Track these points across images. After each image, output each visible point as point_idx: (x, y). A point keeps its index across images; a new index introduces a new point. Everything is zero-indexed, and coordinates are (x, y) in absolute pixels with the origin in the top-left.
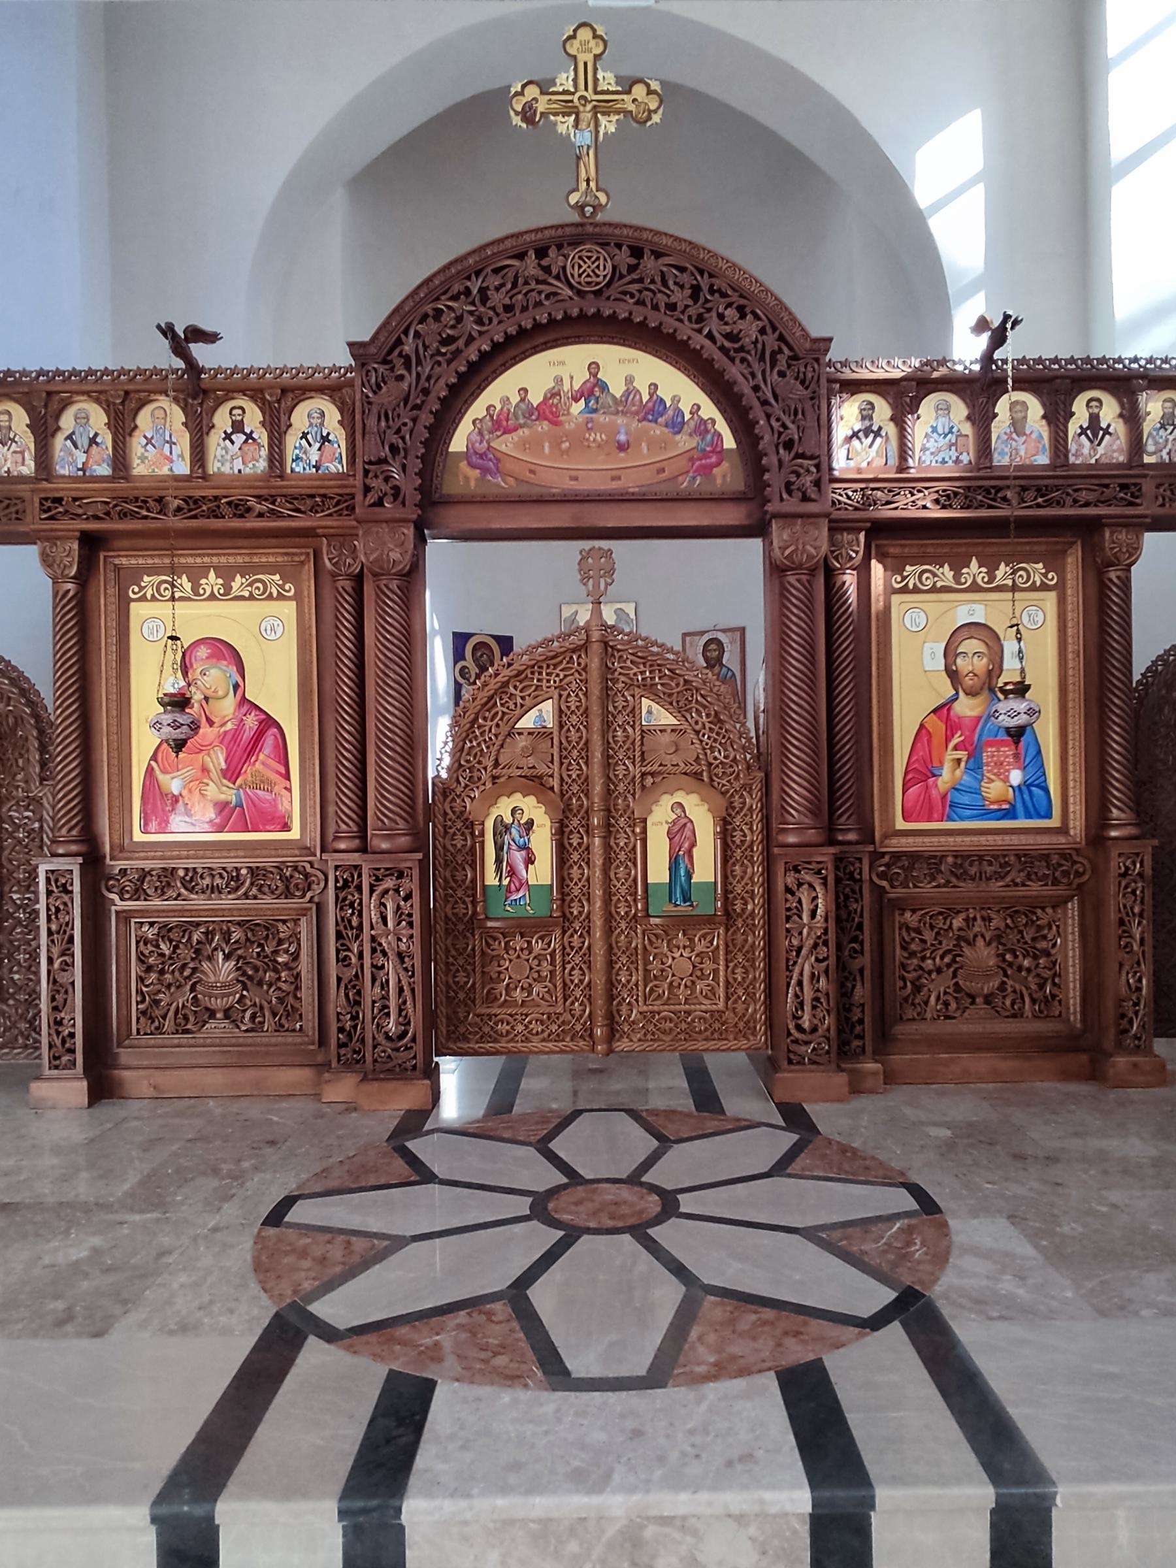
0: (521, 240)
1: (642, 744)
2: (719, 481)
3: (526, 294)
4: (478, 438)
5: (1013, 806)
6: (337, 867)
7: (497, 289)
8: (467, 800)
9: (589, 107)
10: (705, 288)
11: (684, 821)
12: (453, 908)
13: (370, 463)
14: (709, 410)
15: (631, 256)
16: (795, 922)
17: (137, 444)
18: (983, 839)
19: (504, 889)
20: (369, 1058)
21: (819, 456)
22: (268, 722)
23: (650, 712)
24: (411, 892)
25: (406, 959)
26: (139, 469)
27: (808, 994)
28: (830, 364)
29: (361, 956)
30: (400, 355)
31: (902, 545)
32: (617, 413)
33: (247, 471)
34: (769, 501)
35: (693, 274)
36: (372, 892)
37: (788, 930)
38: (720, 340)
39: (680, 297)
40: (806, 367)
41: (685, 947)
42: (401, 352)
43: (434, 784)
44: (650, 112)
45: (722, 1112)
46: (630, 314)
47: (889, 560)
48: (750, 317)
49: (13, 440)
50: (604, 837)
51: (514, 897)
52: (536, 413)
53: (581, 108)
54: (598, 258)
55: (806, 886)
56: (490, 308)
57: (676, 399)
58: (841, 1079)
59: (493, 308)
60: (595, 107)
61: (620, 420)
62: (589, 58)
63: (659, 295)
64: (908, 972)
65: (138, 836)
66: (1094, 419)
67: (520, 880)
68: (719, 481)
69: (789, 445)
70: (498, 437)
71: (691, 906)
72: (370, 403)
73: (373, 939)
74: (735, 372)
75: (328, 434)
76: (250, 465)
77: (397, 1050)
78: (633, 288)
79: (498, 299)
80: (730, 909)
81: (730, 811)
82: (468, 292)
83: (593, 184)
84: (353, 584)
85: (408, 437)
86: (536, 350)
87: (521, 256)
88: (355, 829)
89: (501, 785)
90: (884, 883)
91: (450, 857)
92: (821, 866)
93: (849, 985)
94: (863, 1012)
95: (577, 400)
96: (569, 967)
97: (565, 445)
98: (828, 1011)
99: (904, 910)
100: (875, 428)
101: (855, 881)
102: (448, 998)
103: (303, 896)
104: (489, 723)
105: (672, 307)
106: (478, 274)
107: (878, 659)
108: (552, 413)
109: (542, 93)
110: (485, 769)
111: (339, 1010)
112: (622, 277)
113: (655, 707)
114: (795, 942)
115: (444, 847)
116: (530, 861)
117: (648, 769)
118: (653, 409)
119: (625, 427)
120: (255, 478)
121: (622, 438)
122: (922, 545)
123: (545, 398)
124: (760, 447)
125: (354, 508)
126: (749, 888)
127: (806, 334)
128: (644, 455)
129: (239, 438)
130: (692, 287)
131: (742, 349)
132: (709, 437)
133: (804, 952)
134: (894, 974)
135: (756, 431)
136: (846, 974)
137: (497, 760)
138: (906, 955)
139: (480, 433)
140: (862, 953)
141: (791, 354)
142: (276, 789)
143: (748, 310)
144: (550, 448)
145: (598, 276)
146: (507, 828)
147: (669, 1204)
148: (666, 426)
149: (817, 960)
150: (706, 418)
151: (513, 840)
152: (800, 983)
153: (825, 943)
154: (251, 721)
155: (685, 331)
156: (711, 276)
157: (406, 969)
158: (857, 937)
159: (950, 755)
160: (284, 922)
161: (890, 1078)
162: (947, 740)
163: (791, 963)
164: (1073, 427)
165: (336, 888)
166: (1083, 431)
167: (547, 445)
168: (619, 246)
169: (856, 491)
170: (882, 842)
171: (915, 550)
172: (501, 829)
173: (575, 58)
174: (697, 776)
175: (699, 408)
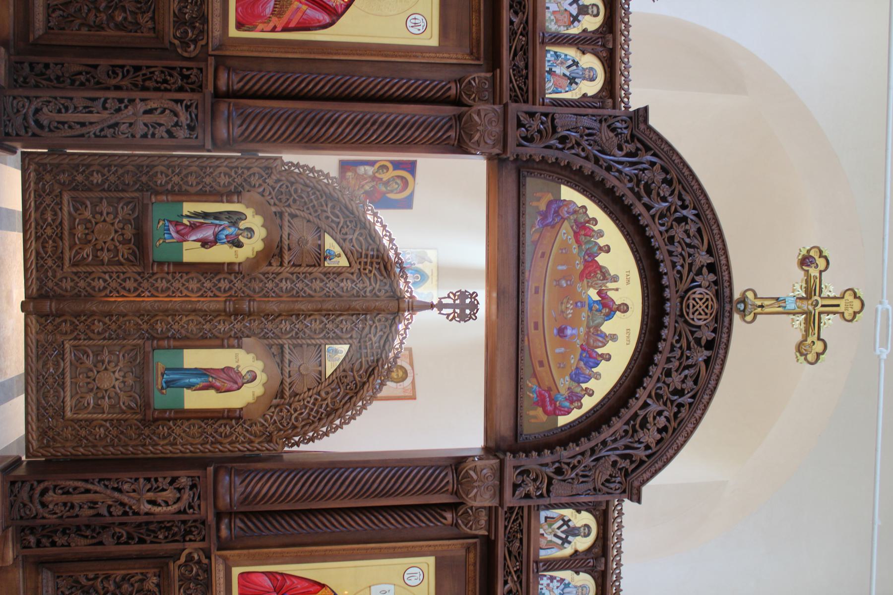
0: (721, 252)
1: (308, 345)
2: (532, 413)
3: (681, 254)
4: (571, 210)
6: (201, 70)
7: (686, 232)
8: (261, 190)
9: (811, 308)
10: (680, 400)
11: (240, 381)
12: (162, 173)
13: (553, 119)
14: (588, 403)
15: (707, 340)
16: (145, 485)
19: (178, 219)
20: (16, 92)
21: (549, 496)
24: (174, 137)
25: (112, 130)
27: (77, 499)
28: (621, 501)
29: (118, 88)
30: (638, 149)
31: (475, 563)
32: (588, 327)
33: (548, 14)
34: (514, 457)
35: (691, 390)
36: (177, 101)
37: (137, 479)
38: (642, 413)
39: (676, 380)
40: (619, 483)
41: (124, 382)
42: (641, 150)
43: (276, 159)
44: (806, 355)
46: (665, 340)
47: (464, 554)
48: (658, 436)
50: (225, 311)
51: (172, 229)
52: (590, 259)
53: (810, 302)
54: (706, 314)
55: (178, 495)
56: (672, 225)
57: (598, 376)
59: (672, 227)
60: (811, 312)
61: (582, 330)
62: (841, 309)
63: (677, 363)
64: (102, 582)
67: (187, 234)
68: (532, 413)
69: (559, 471)
70: (572, 227)
71: (162, 388)
72: (601, 122)
74: (618, 425)
75: (577, 84)
76: (552, 17)
77: (25, 118)
78: (684, 343)
79: (678, 232)
80: (160, 422)
81: (248, 423)
82: (684, 207)
83: (759, 310)
84: (453, 97)
85: (573, 151)
86: (638, 261)
88: (235, 87)
89: (273, 220)
90: (183, 559)
91: (208, 170)
92: (196, 508)
93: (88, 533)
94: (63, 545)
95: (599, 293)
96: (107, 277)
97: (564, 283)
98: (62, 517)
99: (159, 576)
100: (570, 538)
101: (184, 536)
102: (78, 165)
103: (175, 37)
104: (329, 210)
105: (668, 374)
106: (697, 215)
107: (380, 549)
108: (590, 273)
109: (821, 272)
110: (289, 206)
111: (66, 65)
112: (692, 333)
113: (341, 356)
114: (126, 487)
115: (218, 167)
117: (287, 351)
118: (590, 357)
119: (577, 334)
121: (569, 332)
122: (475, 580)
123: (600, 268)
124: (558, 448)
125: (516, 101)
126: (179, 440)
127: (644, 482)
128: (555, 350)
129: (574, 10)
130: (683, 390)
131: (635, 431)
132: (567, 404)
133: (116, 494)
134: (100, 570)
135: (571, 444)
136: (98, 529)
137: (296, 216)
138: (117, 580)
139: (575, 212)
140: (118, 544)
141: (630, 470)
142: (274, 19)
143: (664, 434)
144: (562, 271)
145: (693, 314)
146: (234, 224)
148: (577, 368)
149: (110, 506)
150: (582, 401)
151: (223, 229)
152: (87, 491)
153: (125, 513)
155: (649, 383)
156: (690, 404)
157: (102, 130)
158: (133, 539)
160: (153, 19)
163: (107, 483)
165: (182, 68)
167: (564, 268)
168: (714, 331)
169: (520, 526)
170: (220, 556)
171: (471, 574)
172: (235, 218)
173: (843, 298)
174: (280, 394)
175: (591, 395)
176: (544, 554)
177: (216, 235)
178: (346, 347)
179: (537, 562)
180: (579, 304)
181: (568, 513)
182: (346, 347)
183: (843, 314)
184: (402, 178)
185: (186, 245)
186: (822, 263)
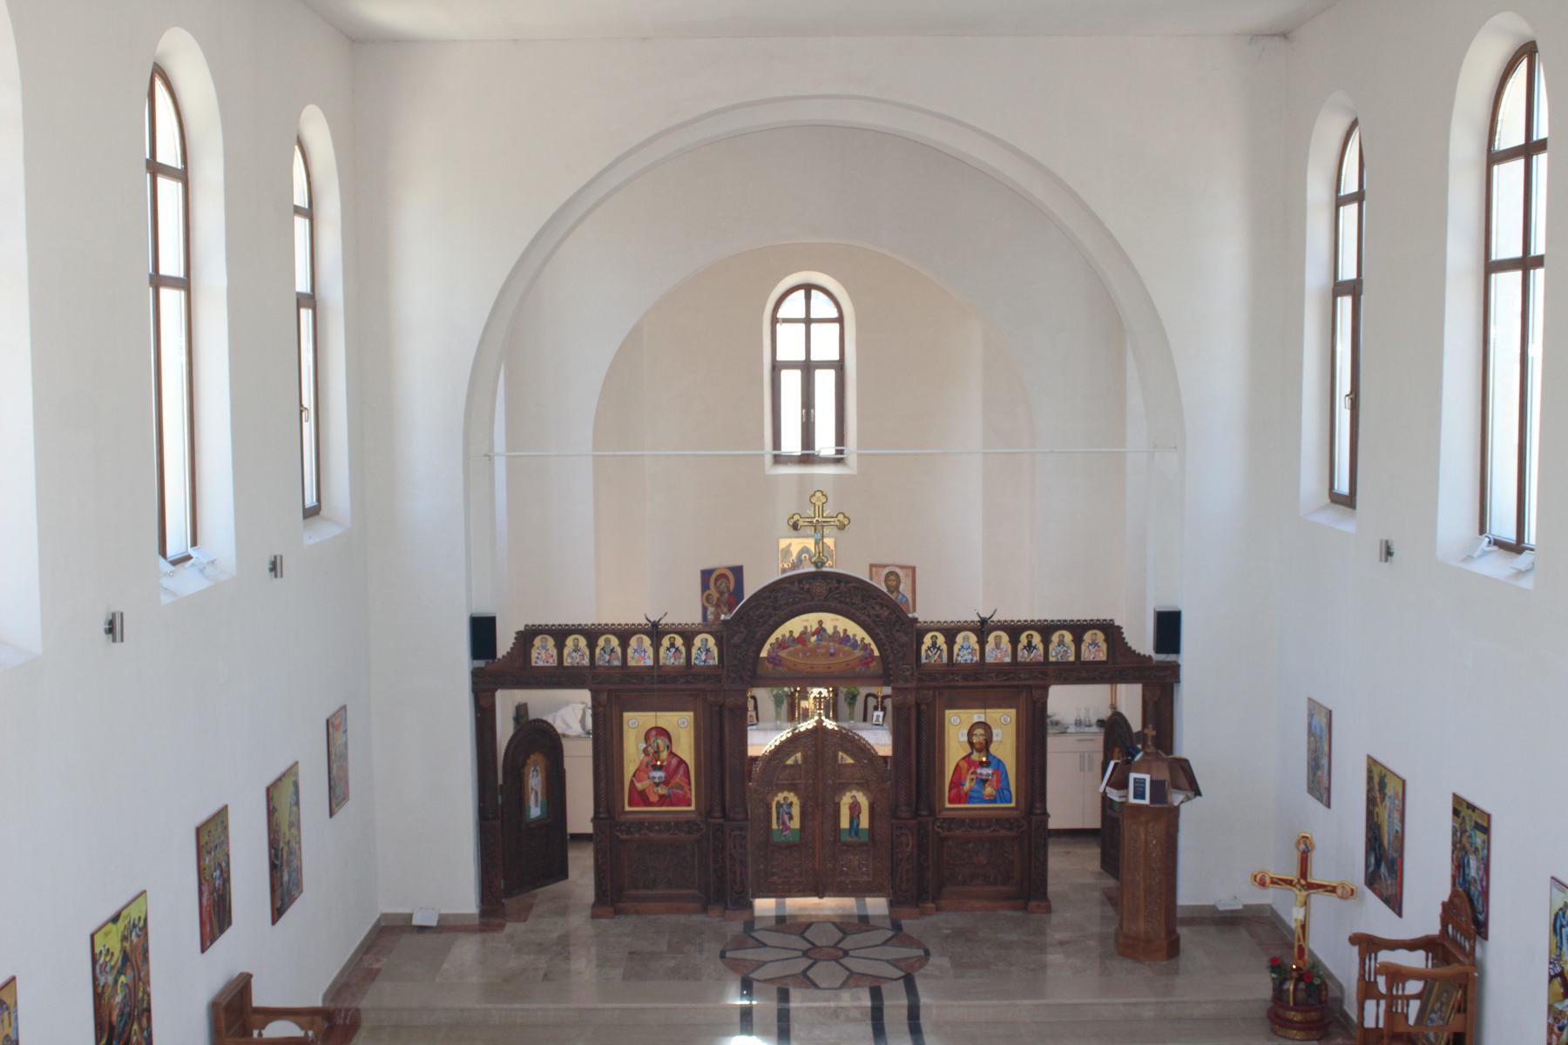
5: (996, 798)
14: (868, 640)
17: (630, 651)
18: (982, 812)
22: (681, 762)
23: (842, 758)
26: (631, 663)
33: (676, 663)
45: (868, 923)
49: (579, 650)
57: (855, 635)
58: (917, 910)
61: (831, 644)
62: (820, 504)
65: (627, 808)
66: (1030, 643)
73: (730, 855)
87: (792, 583)
89: (781, 789)
90: (940, 830)
97: (808, 654)
113: (845, 756)
116: (791, 818)
120: (680, 667)
121: (832, 651)
128: (841, 658)
129: (673, 650)
131: (882, 621)
132: (868, 651)
147: (846, 953)
154: (674, 761)
159: (969, 777)
161: (938, 909)
162: (968, 770)
164: (1020, 646)
166: (1025, 647)
172: (779, 805)
176: (945, 659)
177: (787, 813)
178: (840, 754)
179: (948, 664)
180: (818, 646)
181: (924, 648)
182: (840, 754)
183: (823, 503)
184: (716, 580)
185: (792, 827)
186: (796, 517)
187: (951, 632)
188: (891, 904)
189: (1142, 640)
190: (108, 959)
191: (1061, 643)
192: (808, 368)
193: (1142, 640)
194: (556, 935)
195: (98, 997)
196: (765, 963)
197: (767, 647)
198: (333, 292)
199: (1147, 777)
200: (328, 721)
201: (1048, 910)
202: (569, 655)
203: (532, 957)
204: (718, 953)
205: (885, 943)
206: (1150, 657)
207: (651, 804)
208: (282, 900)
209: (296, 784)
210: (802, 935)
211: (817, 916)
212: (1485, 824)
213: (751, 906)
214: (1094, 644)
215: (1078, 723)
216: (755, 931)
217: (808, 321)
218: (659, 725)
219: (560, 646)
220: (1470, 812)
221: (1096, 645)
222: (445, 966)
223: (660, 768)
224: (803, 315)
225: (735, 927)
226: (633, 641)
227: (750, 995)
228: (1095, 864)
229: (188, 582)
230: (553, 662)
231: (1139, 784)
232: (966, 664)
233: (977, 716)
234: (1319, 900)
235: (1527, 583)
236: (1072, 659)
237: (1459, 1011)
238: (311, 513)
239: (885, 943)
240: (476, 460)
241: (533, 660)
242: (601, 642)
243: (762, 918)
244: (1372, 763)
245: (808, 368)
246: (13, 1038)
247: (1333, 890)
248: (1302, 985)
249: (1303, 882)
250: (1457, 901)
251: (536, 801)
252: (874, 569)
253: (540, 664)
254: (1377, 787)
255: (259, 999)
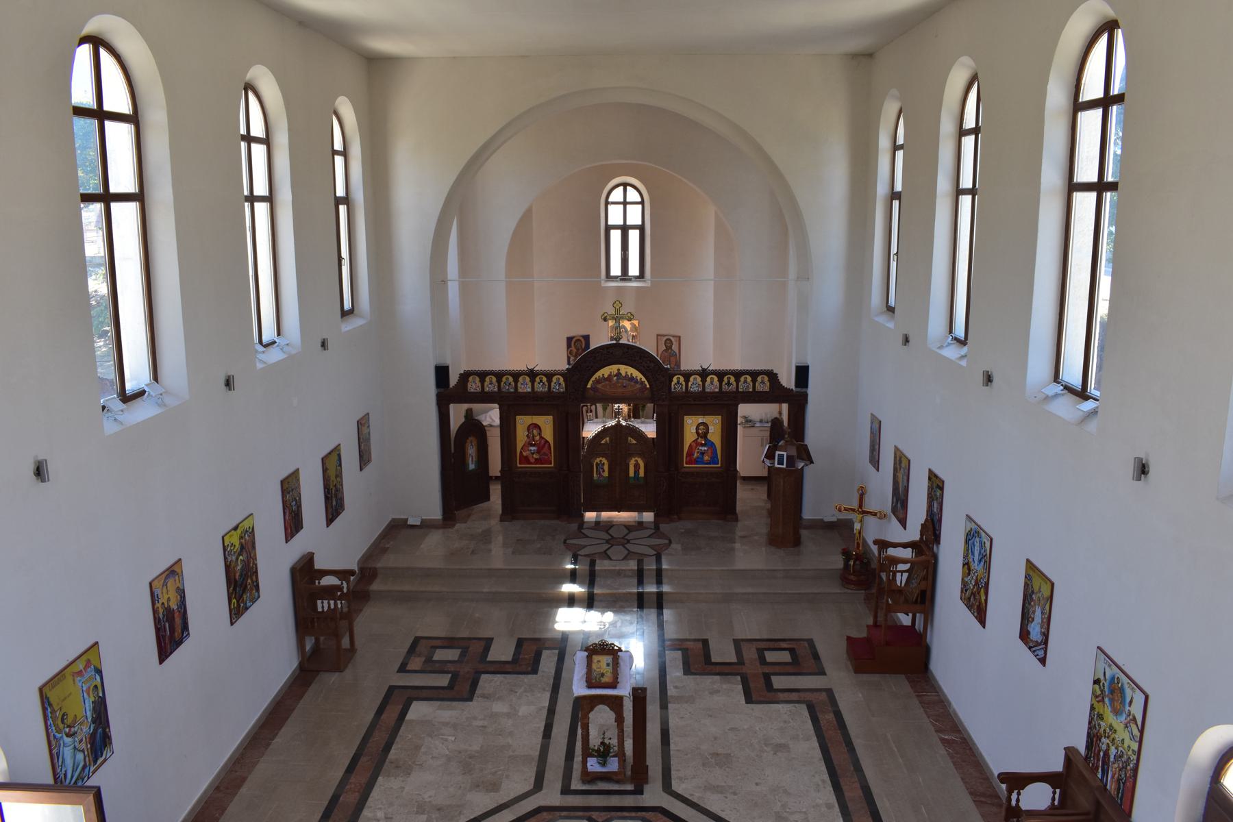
14: (644, 379)
17: (519, 385)
22: (547, 442)
26: (520, 390)
57: (636, 377)
65: (519, 465)
66: (729, 381)
105: (635, 361)
116: (604, 471)
147: (628, 541)
154: (543, 441)
159: (696, 451)
161: (679, 519)
164: (724, 383)
172: (597, 464)
176: (684, 390)
181: (673, 383)
184: (575, 342)
187: (687, 376)
188: (655, 516)
189: (788, 380)
190: (232, 548)
191: (745, 382)
192: (625, 229)
193: (788, 380)
194: (480, 530)
195: (228, 568)
196: (585, 546)
197: (590, 382)
198: (359, 196)
199: (785, 454)
200: (358, 422)
201: (736, 520)
202: (487, 386)
203: (467, 542)
204: (562, 540)
205: (649, 537)
206: (792, 389)
207: (531, 463)
208: (332, 515)
209: (339, 456)
210: (607, 532)
211: (617, 521)
212: (941, 486)
213: (582, 516)
214: (763, 382)
215: (761, 421)
216: (582, 529)
217: (625, 203)
218: (534, 422)
219: (482, 381)
220: (935, 479)
221: (764, 383)
222: (422, 546)
223: (534, 445)
224: (622, 200)
225: (574, 526)
226: (521, 379)
227: (575, 563)
228: (765, 496)
229: (274, 356)
230: (479, 390)
231: (781, 457)
232: (695, 392)
233: (701, 419)
234: (870, 520)
235: (963, 363)
236: (751, 390)
237: (924, 579)
238: (345, 314)
239: (649, 537)
240: (438, 282)
241: (469, 388)
242: (504, 379)
243: (587, 522)
244: (897, 449)
245: (625, 229)
246: (181, 588)
247: (875, 514)
248: (857, 562)
249: (860, 510)
250: (927, 523)
251: (472, 461)
252: (659, 337)
253: (472, 390)
254: (898, 462)
255: (319, 564)
